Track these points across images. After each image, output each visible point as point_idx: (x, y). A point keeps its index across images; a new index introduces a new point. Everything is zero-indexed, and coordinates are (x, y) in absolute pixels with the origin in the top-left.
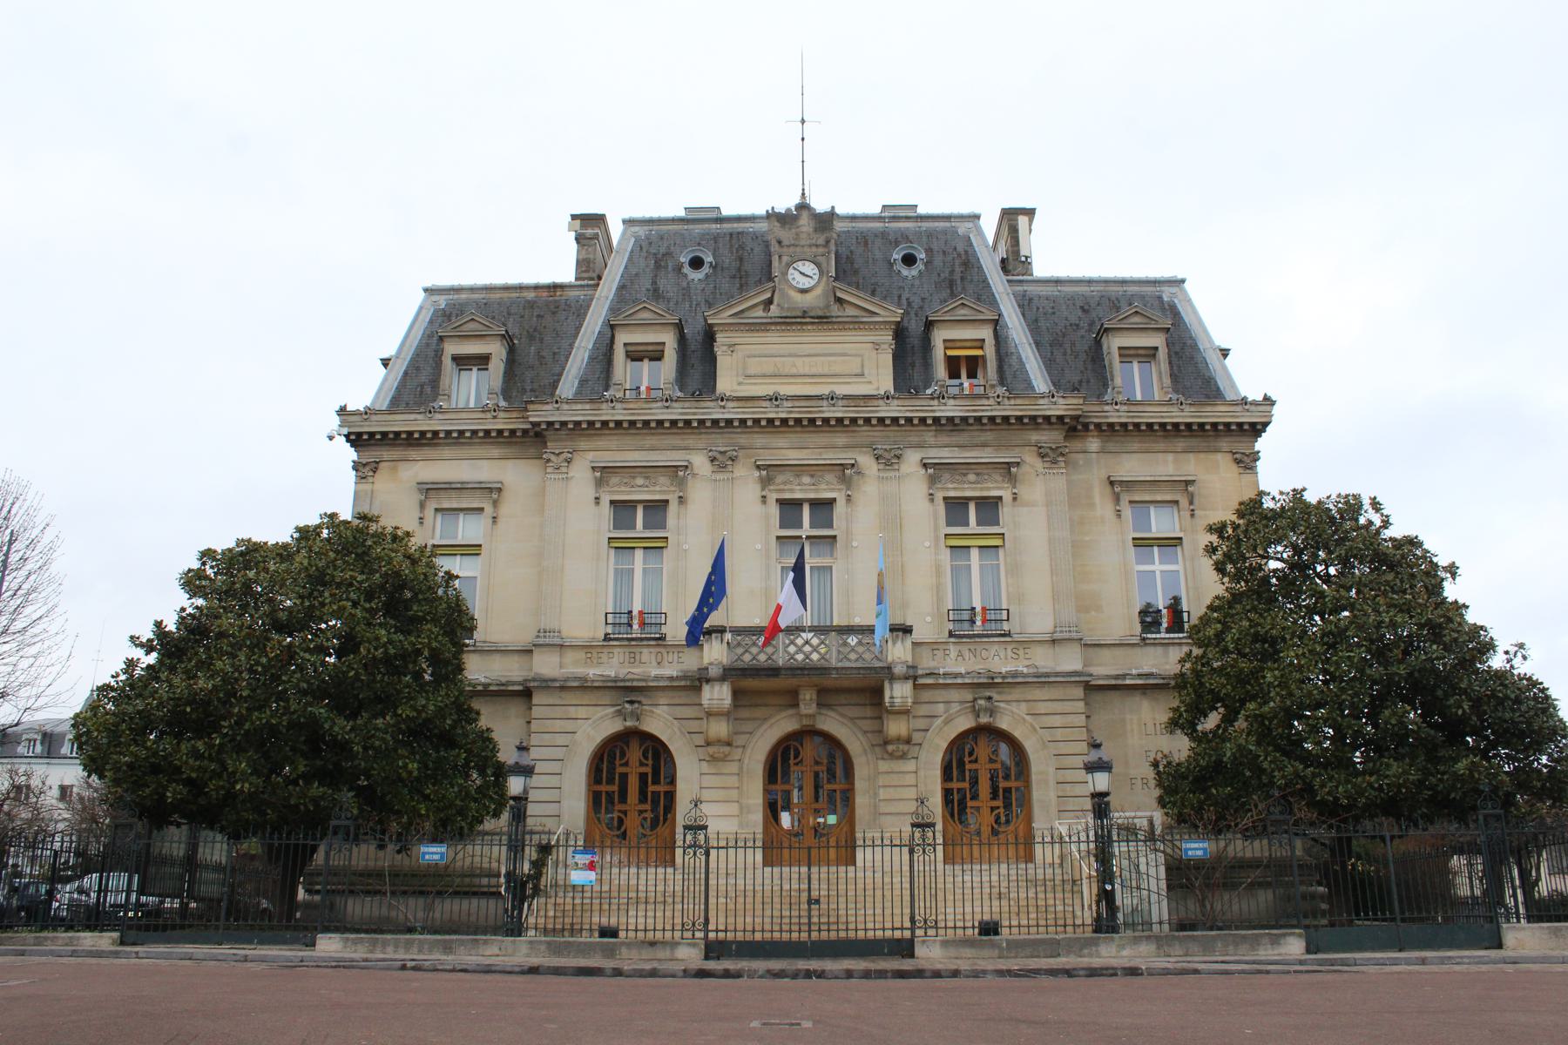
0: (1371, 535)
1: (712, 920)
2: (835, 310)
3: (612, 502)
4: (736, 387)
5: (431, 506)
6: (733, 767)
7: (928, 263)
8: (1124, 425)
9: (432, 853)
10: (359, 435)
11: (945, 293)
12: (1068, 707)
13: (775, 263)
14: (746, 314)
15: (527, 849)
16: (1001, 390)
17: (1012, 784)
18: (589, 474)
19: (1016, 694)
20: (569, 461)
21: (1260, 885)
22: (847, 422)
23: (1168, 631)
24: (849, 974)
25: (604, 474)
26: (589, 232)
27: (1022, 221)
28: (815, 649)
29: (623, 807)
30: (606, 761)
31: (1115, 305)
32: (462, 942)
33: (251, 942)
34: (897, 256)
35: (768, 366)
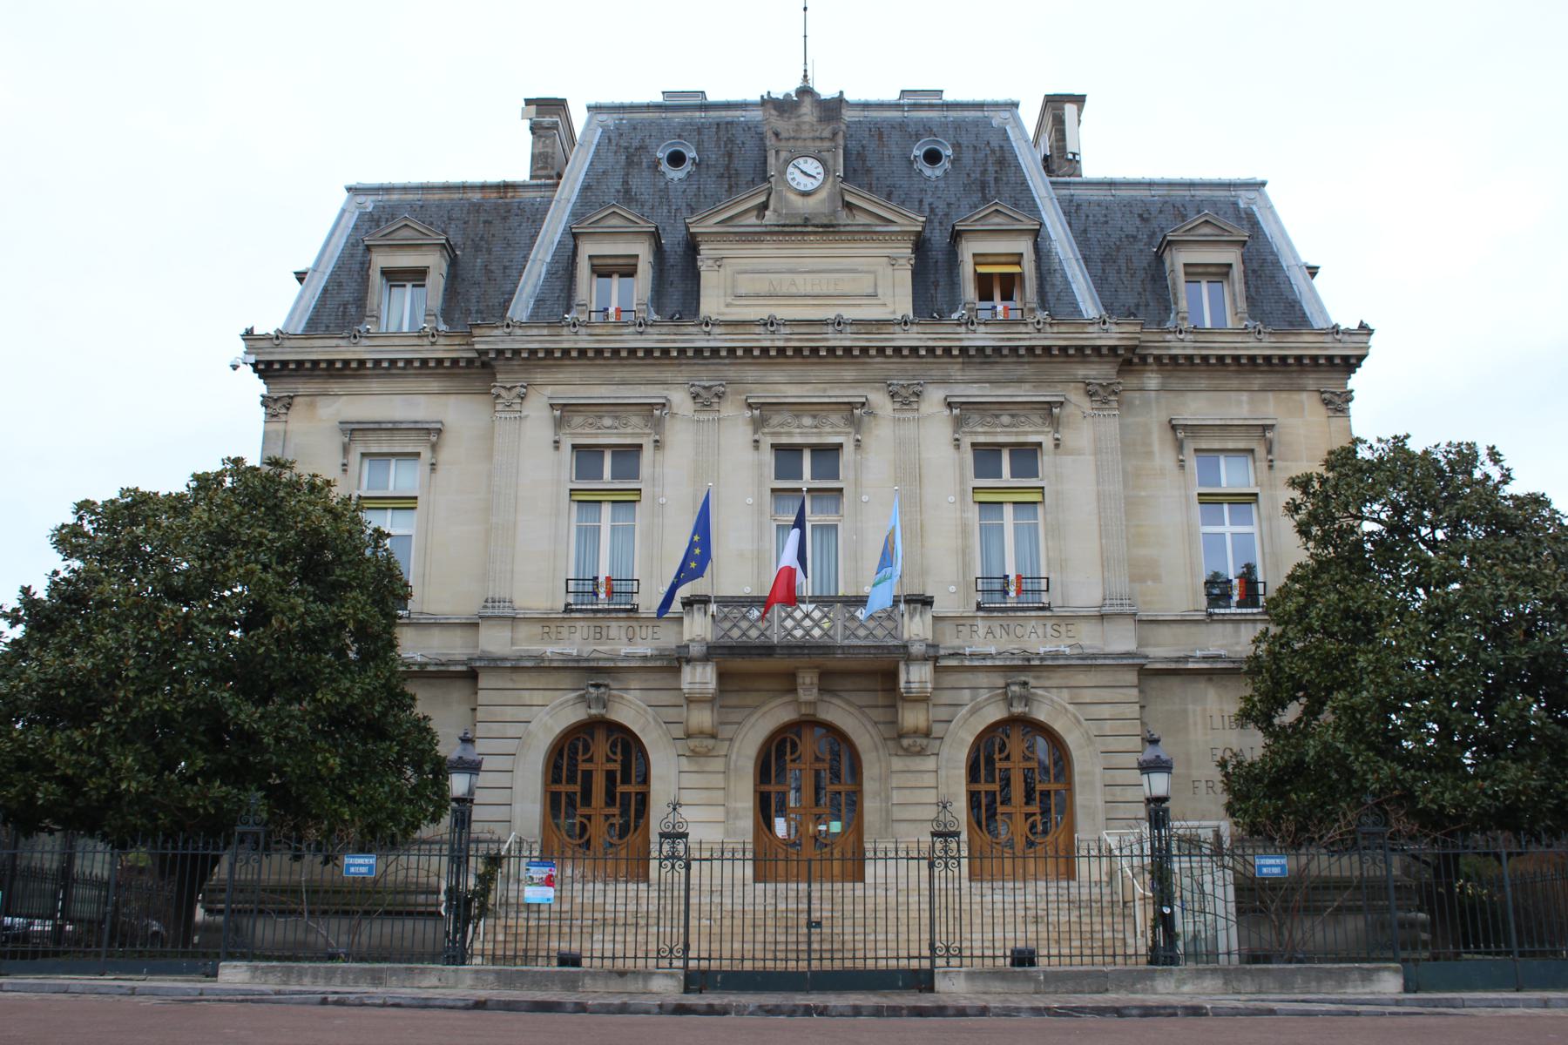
0: (1487, 492)
1: (693, 946)
2: (843, 217)
3: (574, 447)
5: (357, 449)
6: (718, 764)
7: (955, 161)
8: (1190, 358)
9: (359, 865)
10: (269, 363)
12: (1117, 695)
13: (771, 160)
14: (735, 222)
15: (472, 860)
16: (1041, 315)
17: (1052, 787)
18: (546, 413)
19: (1056, 679)
20: (522, 397)
21: (1350, 910)
22: (856, 352)
23: (1239, 605)
24: (857, 1011)
25: (564, 412)
26: (547, 120)
27: (1070, 110)
28: (817, 624)
29: (586, 811)
30: (566, 755)
32: (394, 972)
33: (139, 972)
34: (918, 152)
35: (761, 284)
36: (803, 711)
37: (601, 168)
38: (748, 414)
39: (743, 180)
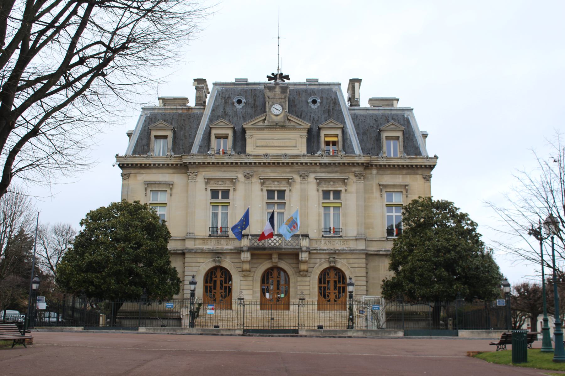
2: (287, 123)
4: (253, 150)
5: (149, 189)
6: (251, 279)
7: (321, 103)
8: (385, 165)
10: (123, 164)
11: (326, 115)
12: (360, 261)
13: (267, 105)
14: (257, 124)
18: (203, 180)
19: (343, 256)
20: (196, 176)
23: (396, 236)
25: (208, 180)
26: (200, 85)
27: (357, 84)
28: (277, 242)
29: (215, 291)
30: (210, 275)
35: (263, 143)
36: (274, 264)
37: (217, 104)
38: (260, 181)
39: (259, 109)
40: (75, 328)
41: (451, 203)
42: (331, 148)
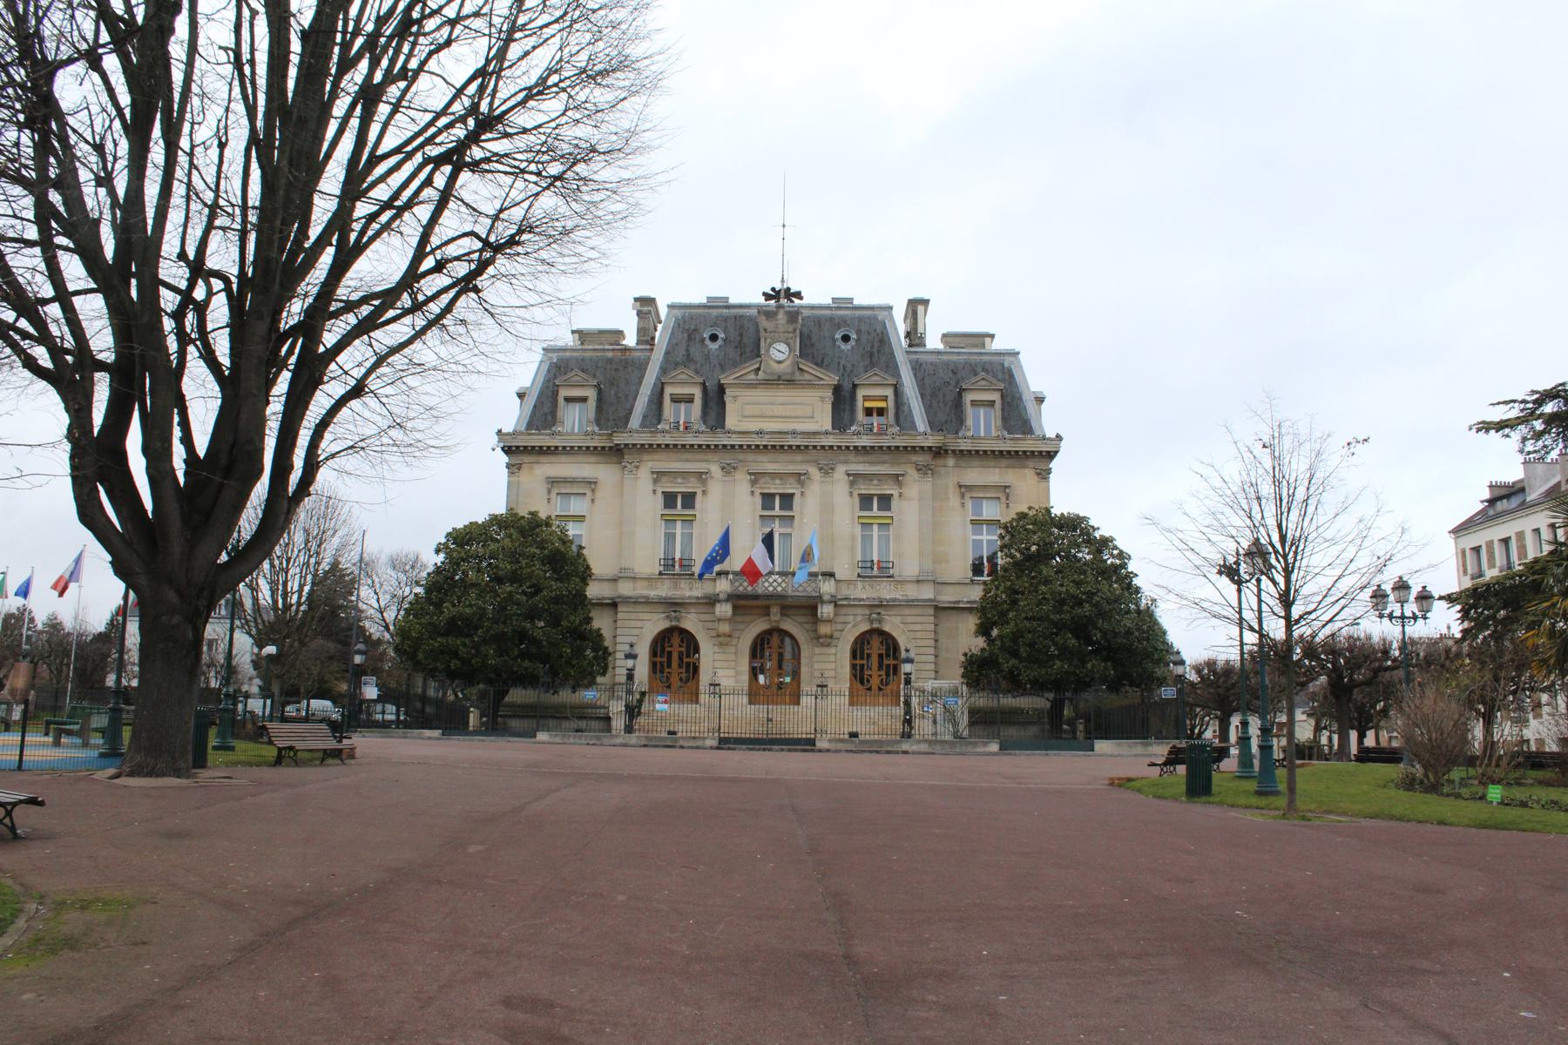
2: (798, 376)
6: (733, 649)
7: (858, 341)
11: (867, 361)
13: (762, 343)
18: (649, 476)
19: (895, 611)
25: (658, 476)
27: (920, 308)
30: (660, 644)
31: (973, 369)
34: (838, 336)
35: (756, 410)
40: (427, 733)
41: (1085, 519)
42: (875, 420)
